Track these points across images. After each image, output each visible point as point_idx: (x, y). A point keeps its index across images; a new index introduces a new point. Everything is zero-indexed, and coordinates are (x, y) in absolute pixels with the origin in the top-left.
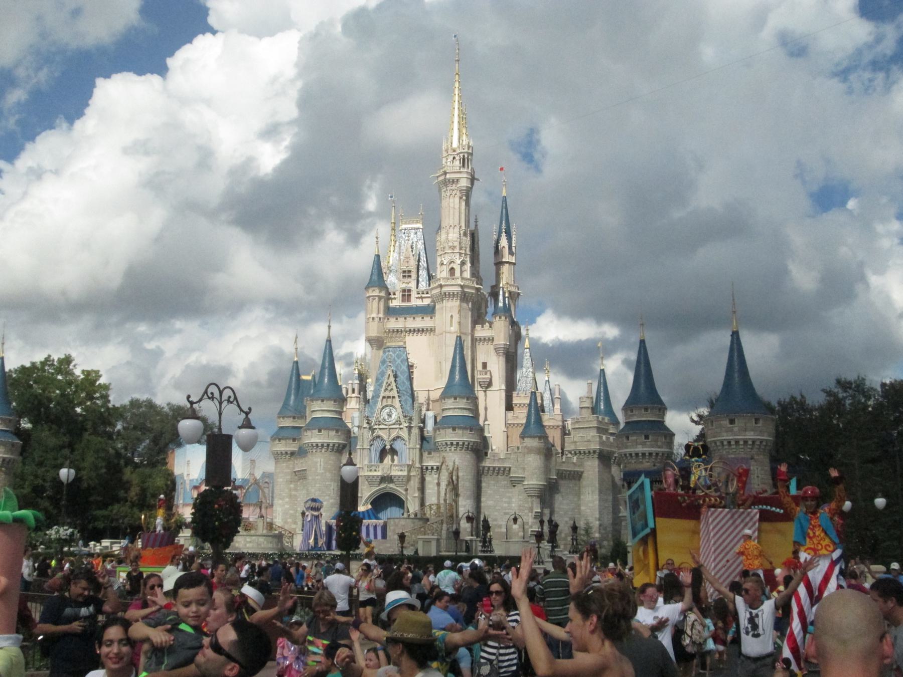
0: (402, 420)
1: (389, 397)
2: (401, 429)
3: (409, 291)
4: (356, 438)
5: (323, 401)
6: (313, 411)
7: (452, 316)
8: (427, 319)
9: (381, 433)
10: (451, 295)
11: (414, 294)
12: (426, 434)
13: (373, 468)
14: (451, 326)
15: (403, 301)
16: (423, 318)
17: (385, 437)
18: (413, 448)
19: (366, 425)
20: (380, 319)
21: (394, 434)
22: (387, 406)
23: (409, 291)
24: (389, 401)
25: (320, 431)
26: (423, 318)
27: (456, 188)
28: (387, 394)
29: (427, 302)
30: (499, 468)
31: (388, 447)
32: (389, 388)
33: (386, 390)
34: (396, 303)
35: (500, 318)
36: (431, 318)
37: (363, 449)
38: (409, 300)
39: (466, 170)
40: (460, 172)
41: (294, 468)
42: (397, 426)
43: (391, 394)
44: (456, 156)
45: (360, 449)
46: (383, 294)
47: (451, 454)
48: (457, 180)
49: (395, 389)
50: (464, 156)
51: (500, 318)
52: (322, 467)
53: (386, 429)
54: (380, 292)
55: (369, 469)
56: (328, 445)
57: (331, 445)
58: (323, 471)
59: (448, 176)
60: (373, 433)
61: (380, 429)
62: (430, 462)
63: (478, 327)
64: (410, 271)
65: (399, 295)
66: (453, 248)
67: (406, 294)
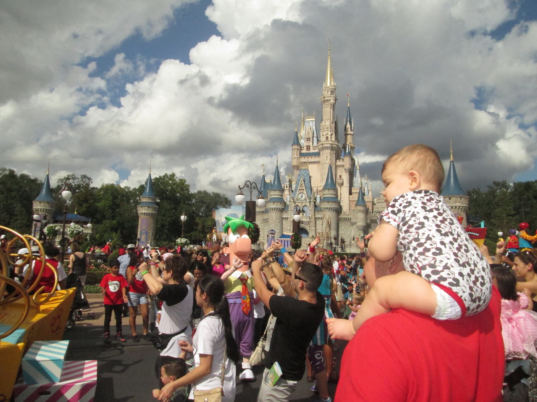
0: (307, 199)
1: (301, 189)
2: (306, 202)
3: (309, 146)
4: (288, 206)
5: (275, 191)
6: (271, 195)
7: (327, 156)
8: (317, 157)
9: (298, 204)
10: (327, 148)
11: (311, 148)
12: (316, 204)
14: (327, 160)
17: (300, 205)
19: (292, 201)
20: (298, 158)
21: (304, 204)
22: (300, 193)
23: (309, 146)
24: (302, 191)
25: (274, 203)
28: (301, 188)
29: (317, 151)
30: (347, 218)
31: (301, 209)
32: (302, 186)
33: (300, 186)
35: (347, 157)
38: (309, 150)
39: (333, 96)
40: (331, 97)
43: (303, 188)
46: (299, 148)
47: (327, 212)
49: (304, 186)
51: (347, 157)
54: (298, 147)
59: (325, 99)
60: (295, 204)
61: (298, 202)
62: (318, 216)
63: (338, 161)
64: (310, 138)
65: (305, 148)
66: (328, 128)
67: (308, 148)
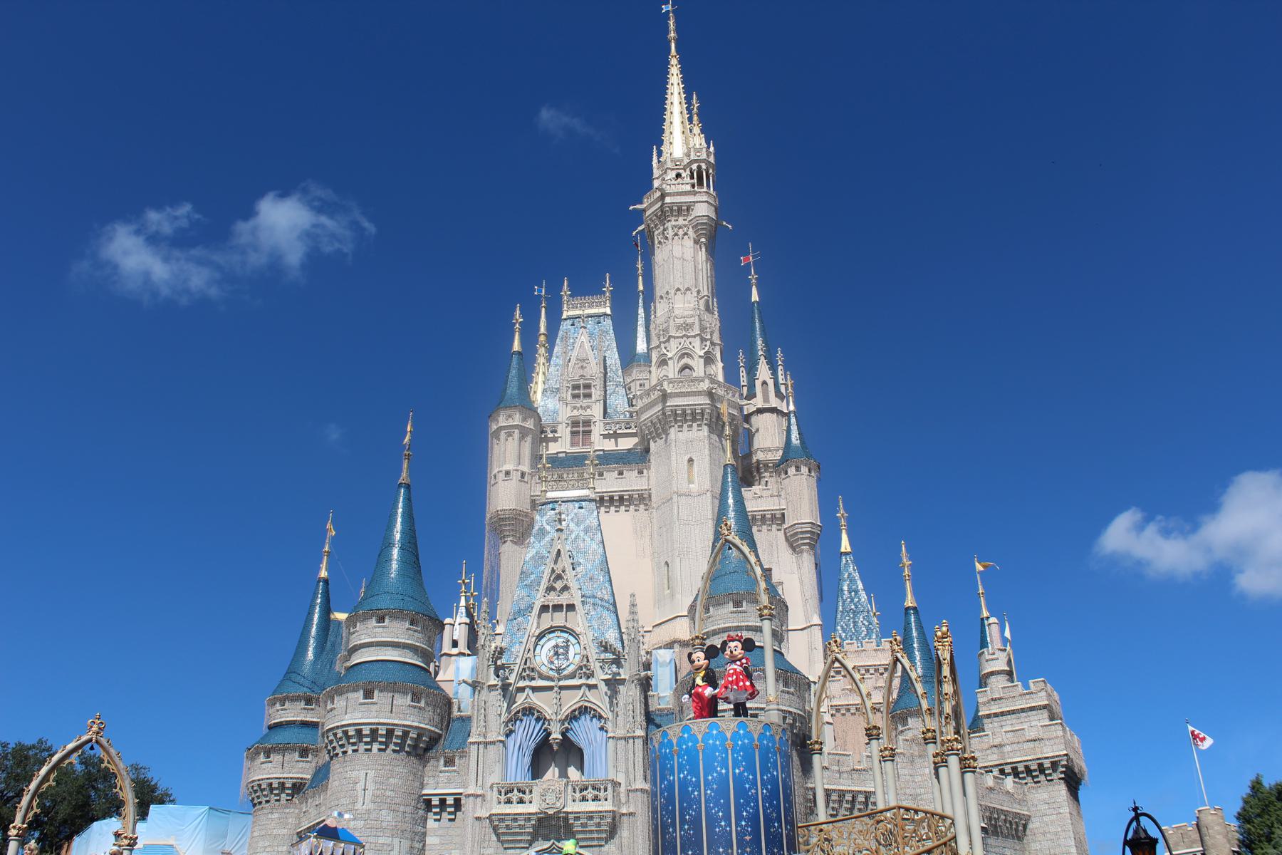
0: (595, 666)
1: (558, 608)
2: (591, 687)
3: (587, 423)
4: (466, 720)
5: (381, 619)
6: (356, 649)
9: (537, 700)
10: (687, 417)
11: (597, 430)
12: (653, 706)
15: (573, 444)
16: (621, 473)
17: (548, 711)
18: (626, 739)
19: (493, 680)
20: (523, 475)
21: (572, 701)
22: (551, 630)
23: (587, 423)
24: (559, 619)
25: (368, 694)
26: (621, 473)
27: (686, 222)
28: (553, 599)
29: (627, 444)
30: (855, 795)
31: (556, 735)
32: (559, 585)
33: (550, 589)
34: (562, 445)
35: (798, 469)
36: (641, 472)
37: (486, 744)
38: (587, 442)
39: (705, 189)
40: (695, 193)
42: (583, 681)
44: (681, 171)
45: (478, 743)
46: (530, 424)
50: (699, 167)
51: (798, 469)
53: (551, 688)
54: (524, 419)
55: (503, 798)
56: (390, 733)
57: (398, 732)
58: (371, 806)
59: (668, 200)
60: (511, 702)
61: (535, 689)
63: (747, 493)
65: (564, 432)
66: (687, 327)
67: (581, 429)
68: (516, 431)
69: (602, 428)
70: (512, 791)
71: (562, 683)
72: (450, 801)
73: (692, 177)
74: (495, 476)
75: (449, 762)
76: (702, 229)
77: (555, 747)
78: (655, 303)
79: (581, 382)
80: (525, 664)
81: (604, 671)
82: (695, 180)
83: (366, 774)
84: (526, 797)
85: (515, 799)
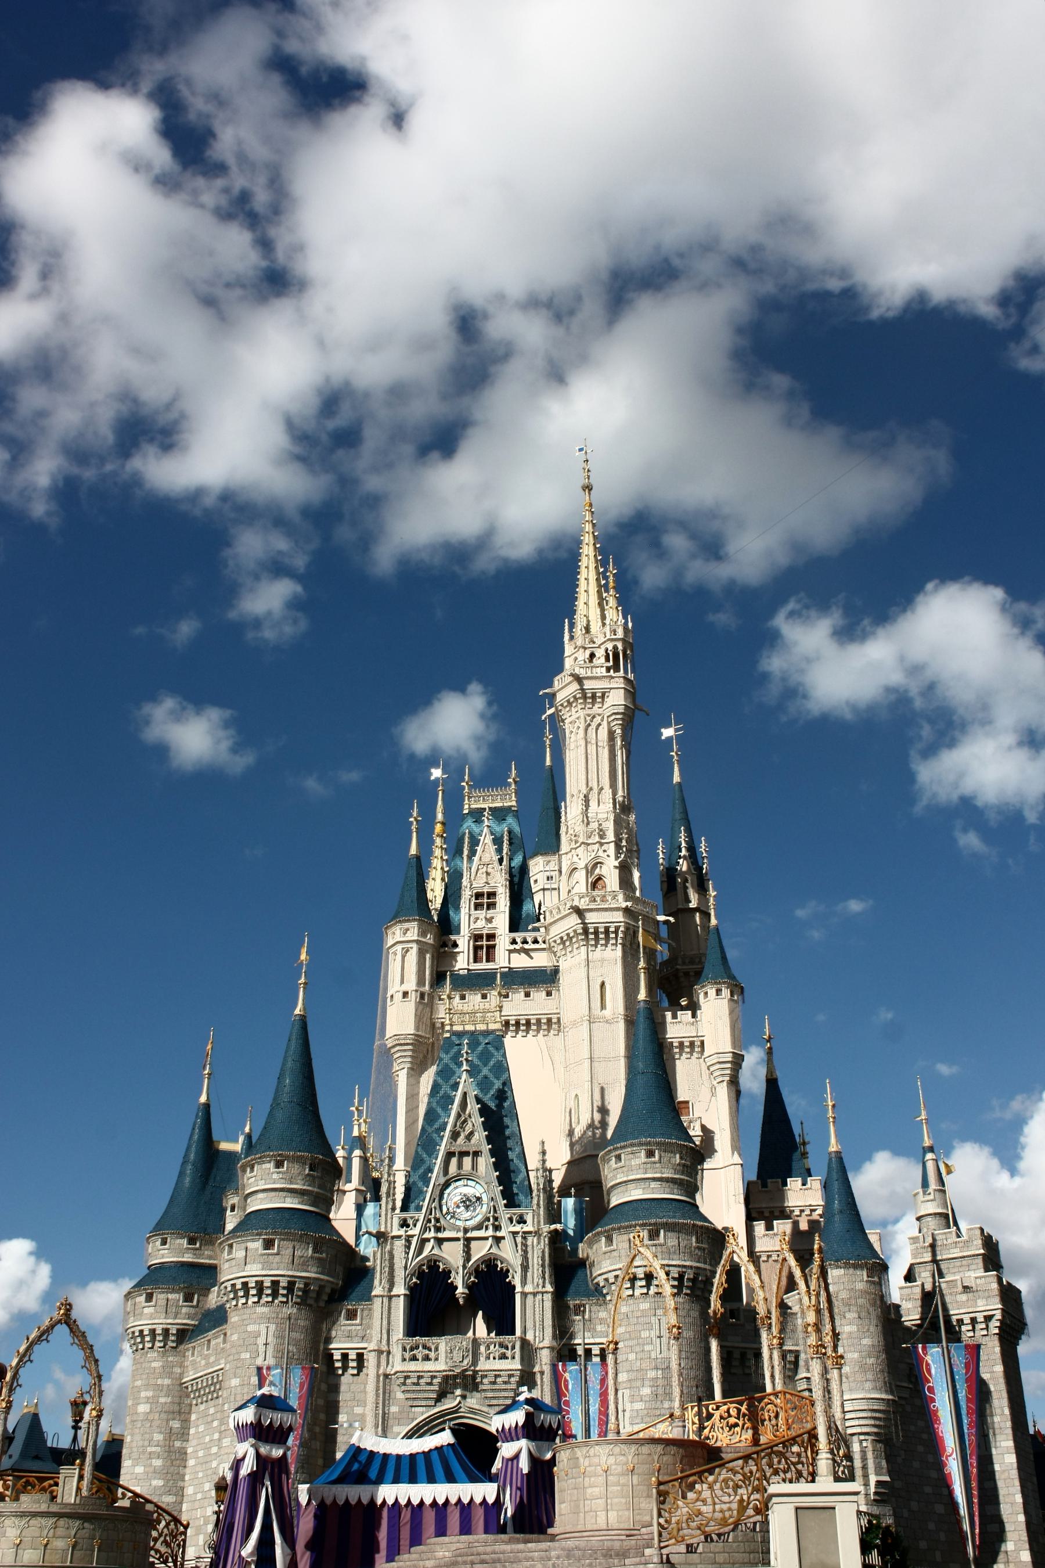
3: (491, 937)
7: (603, 984)
8: (539, 995)
11: (503, 943)
13: (420, 1353)
14: (603, 1006)
16: (527, 995)
23: (491, 937)
26: (527, 995)
35: (718, 992)
36: (549, 994)
41: (182, 1375)
45: (382, 1296)
48: (603, 694)
50: (615, 648)
52: (270, 1349)
53: (457, 1239)
55: (407, 1355)
64: (492, 895)
68: (415, 946)
69: (508, 940)
70: (417, 1347)
71: (469, 1235)
72: (352, 1355)
73: (607, 659)
74: (392, 996)
75: (352, 1315)
76: (617, 719)
77: (461, 1301)
78: (565, 803)
79: (485, 890)
80: (431, 1214)
81: (512, 1222)
82: (611, 663)
83: (267, 1327)
84: (432, 1355)
85: (420, 1357)
